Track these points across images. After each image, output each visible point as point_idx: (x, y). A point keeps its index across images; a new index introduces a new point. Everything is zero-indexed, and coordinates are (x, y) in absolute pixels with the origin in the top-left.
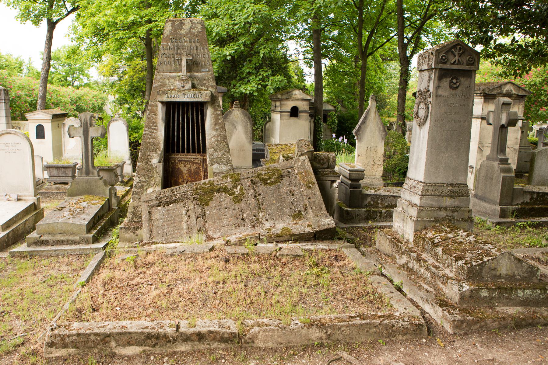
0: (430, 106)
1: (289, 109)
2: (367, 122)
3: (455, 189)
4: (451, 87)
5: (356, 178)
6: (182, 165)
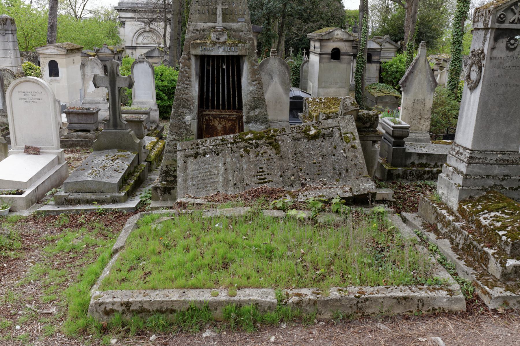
0: (483, 69)
1: (329, 51)
2: (416, 72)
3: (506, 157)
4: (508, 48)
5: (399, 136)
6: (217, 122)
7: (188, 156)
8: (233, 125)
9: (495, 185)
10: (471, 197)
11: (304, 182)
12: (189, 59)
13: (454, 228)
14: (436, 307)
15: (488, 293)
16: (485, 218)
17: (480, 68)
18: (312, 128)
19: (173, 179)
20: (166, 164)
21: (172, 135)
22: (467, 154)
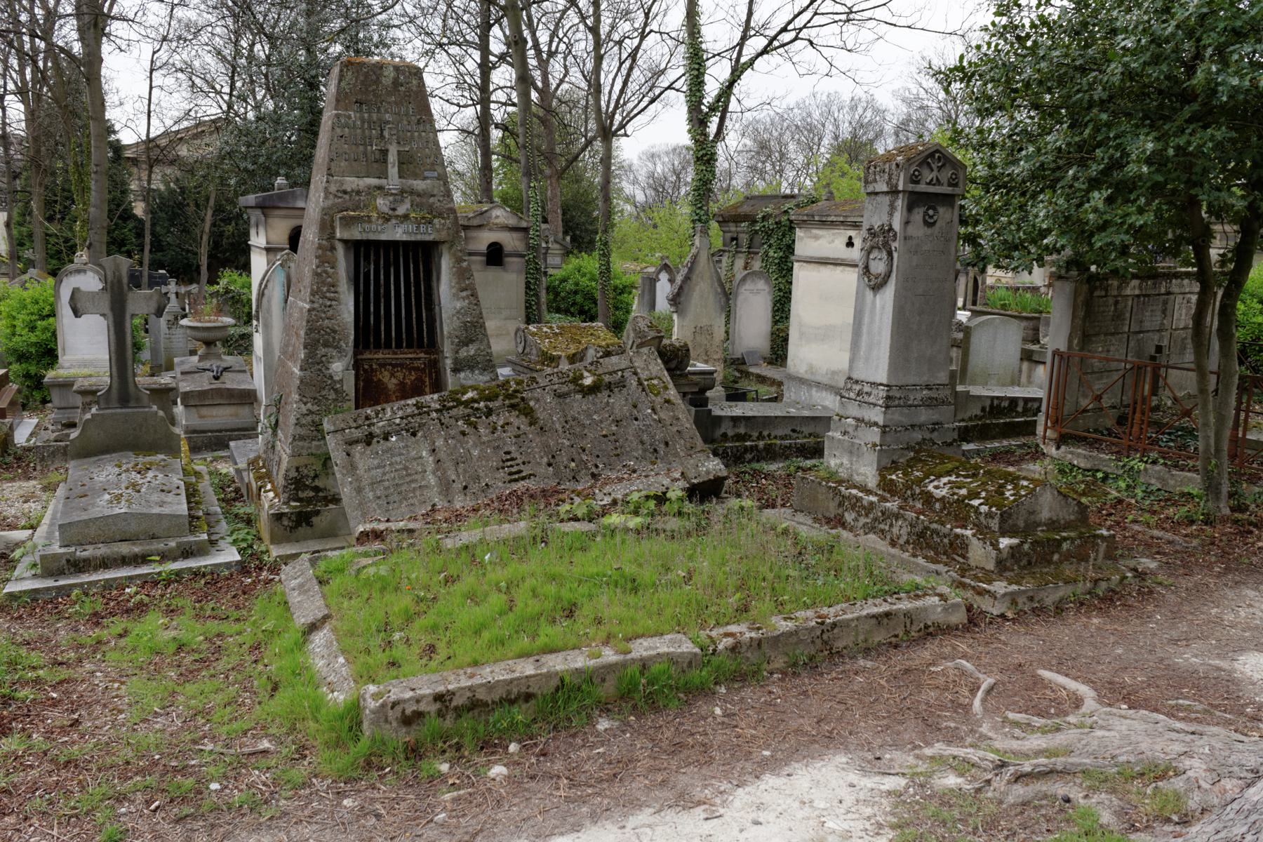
0: (895, 255)
1: (483, 247)
2: (694, 277)
3: (933, 394)
7: (352, 443)
8: (420, 379)
9: (924, 439)
10: (893, 462)
11: (594, 470)
12: (333, 248)
13: (883, 513)
14: (929, 623)
15: (989, 592)
16: (937, 487)
17: (890, 254)
18: (586, 374)
19: (312, 494)
20: (296, 464)
21: (305, 404)
22: (882, 392)
